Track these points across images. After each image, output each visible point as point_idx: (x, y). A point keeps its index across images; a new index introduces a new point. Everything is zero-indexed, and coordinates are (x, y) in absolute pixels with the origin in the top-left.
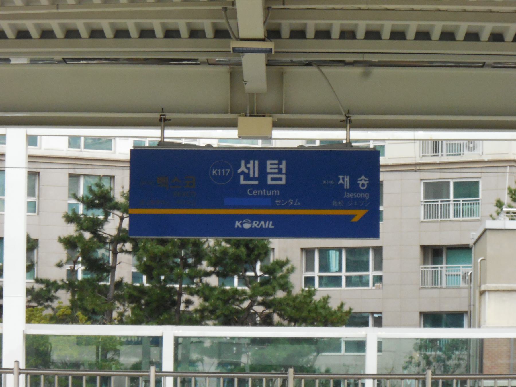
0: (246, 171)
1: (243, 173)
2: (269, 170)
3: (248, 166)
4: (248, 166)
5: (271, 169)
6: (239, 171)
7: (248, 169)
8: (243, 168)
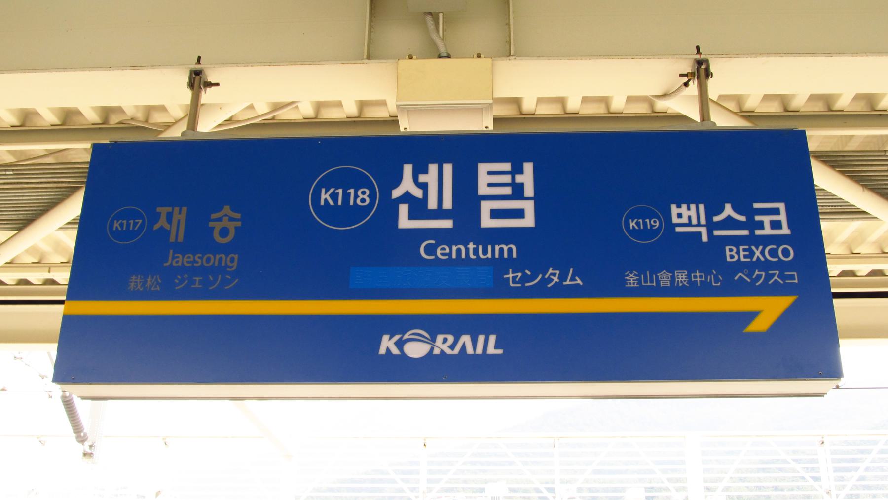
0: (418, 193)
1: (407, 197)
2: (483, 189)
3: (422, 178)
4: (422, 178)
5: (490, 185)
6: (396, 193)
7: (424, 187)
8: (407, 185)
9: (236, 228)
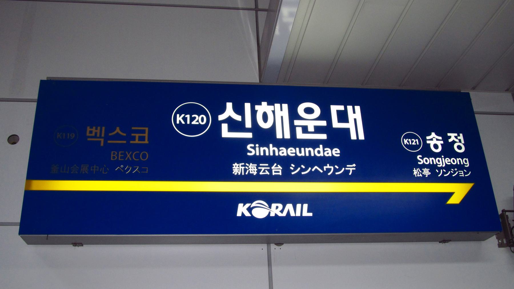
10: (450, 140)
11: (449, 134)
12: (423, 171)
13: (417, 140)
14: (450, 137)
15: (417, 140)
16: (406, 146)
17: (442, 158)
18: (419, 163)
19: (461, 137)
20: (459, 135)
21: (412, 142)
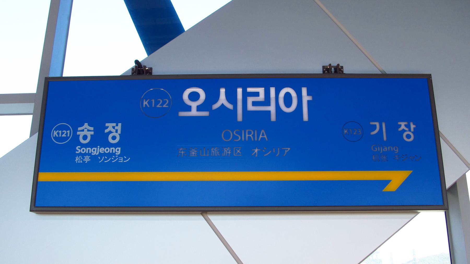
9: (91, 135)
10: (106, 131)
11: (107, 125)
12: (84, 158)
13: (68, 131)
14: (107, 127)
15: (68, 131)
16: (55, 138)
17: (97, 148)
18: (77, 152)
19: (119, 127)
20: (117, 125)
21: (62, 133)
